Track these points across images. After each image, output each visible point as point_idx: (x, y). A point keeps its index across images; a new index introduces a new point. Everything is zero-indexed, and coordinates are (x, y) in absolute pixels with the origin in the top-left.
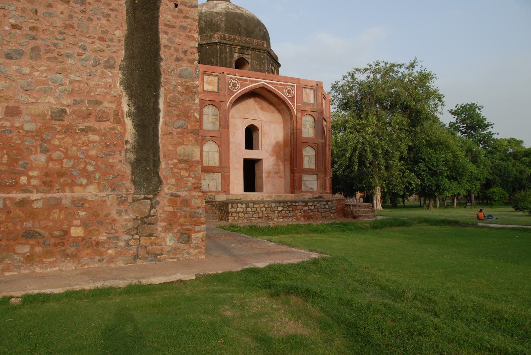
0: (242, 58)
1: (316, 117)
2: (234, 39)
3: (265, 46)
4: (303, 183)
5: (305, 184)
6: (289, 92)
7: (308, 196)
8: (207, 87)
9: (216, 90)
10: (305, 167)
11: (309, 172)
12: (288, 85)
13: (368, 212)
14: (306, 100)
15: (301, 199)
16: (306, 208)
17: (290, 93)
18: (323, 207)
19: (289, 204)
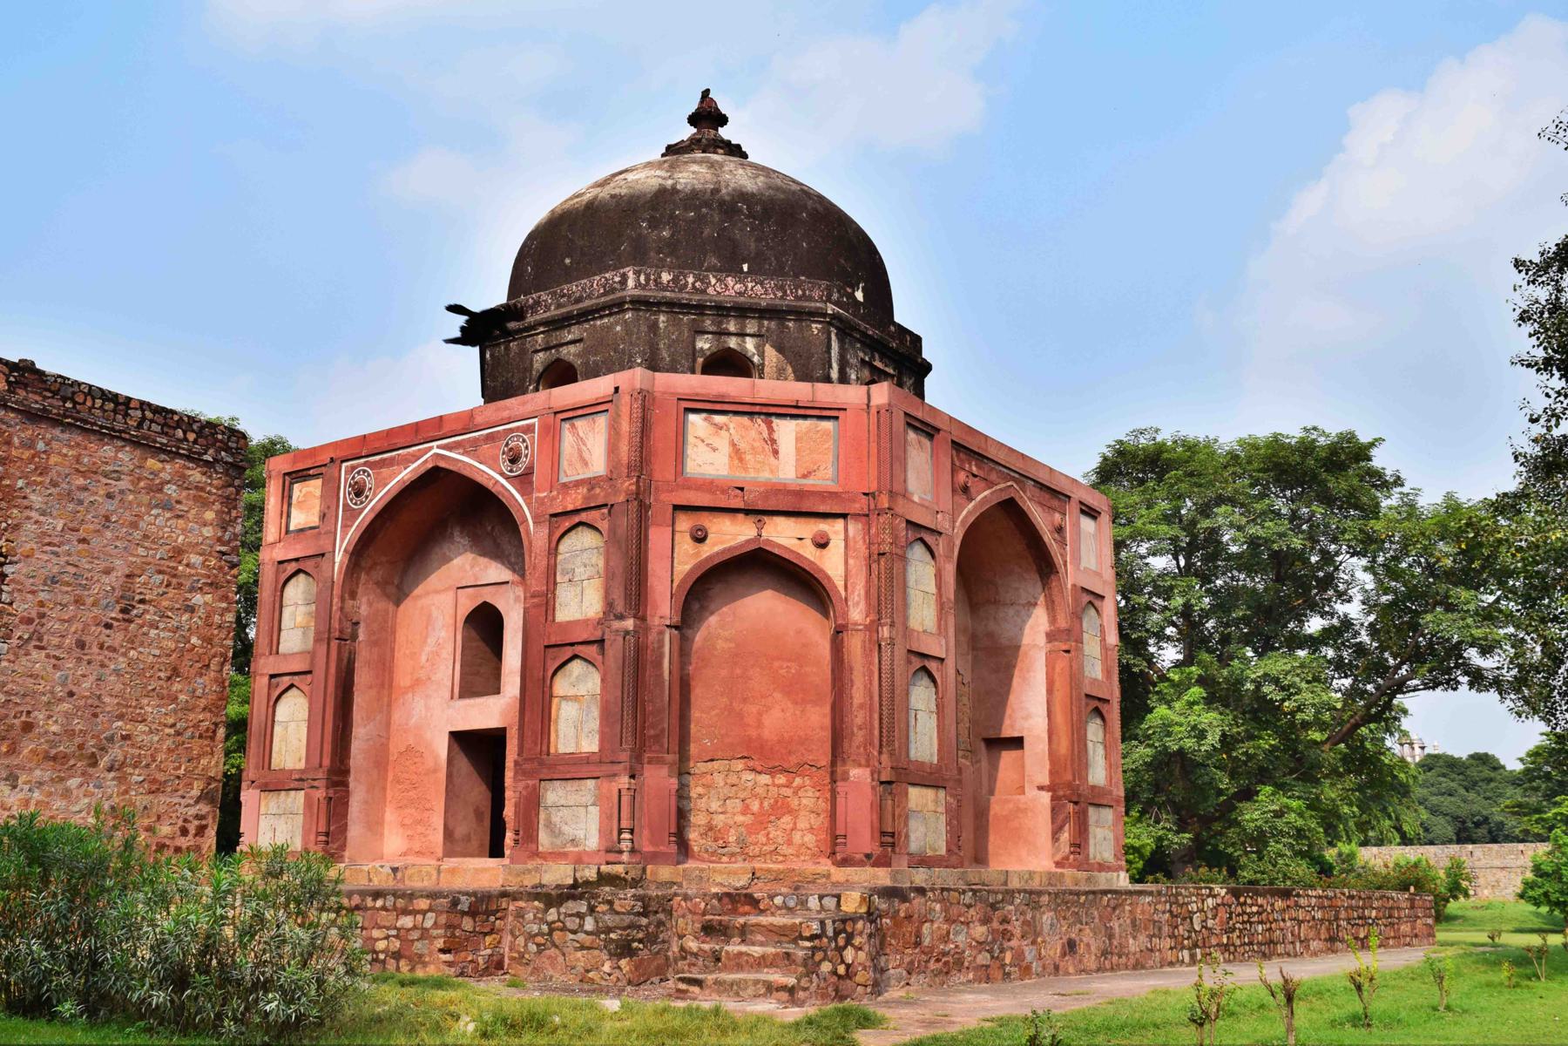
0: (558, 360)
1: (604, 526)
2: (537, 303)
3: (631, 283)
4: (542, 816)
5: (549, 825)
6: (514, 461)
7: (557, 874)
8: (298, 519)
9: (314, 520)
10: (562, 750)
11: (574, 769)
12: (512, 430)
13: (762, 962)
14: (570, 473)
15: (529, 881)
16: (407, 922)
17: (514, 461)
18: (572, 923)
19: (356, 900)
